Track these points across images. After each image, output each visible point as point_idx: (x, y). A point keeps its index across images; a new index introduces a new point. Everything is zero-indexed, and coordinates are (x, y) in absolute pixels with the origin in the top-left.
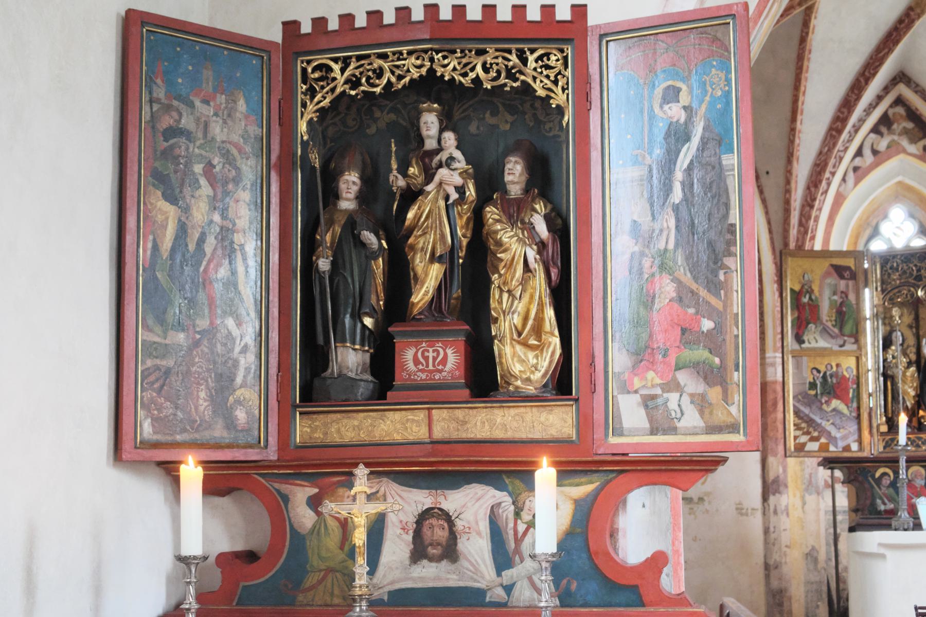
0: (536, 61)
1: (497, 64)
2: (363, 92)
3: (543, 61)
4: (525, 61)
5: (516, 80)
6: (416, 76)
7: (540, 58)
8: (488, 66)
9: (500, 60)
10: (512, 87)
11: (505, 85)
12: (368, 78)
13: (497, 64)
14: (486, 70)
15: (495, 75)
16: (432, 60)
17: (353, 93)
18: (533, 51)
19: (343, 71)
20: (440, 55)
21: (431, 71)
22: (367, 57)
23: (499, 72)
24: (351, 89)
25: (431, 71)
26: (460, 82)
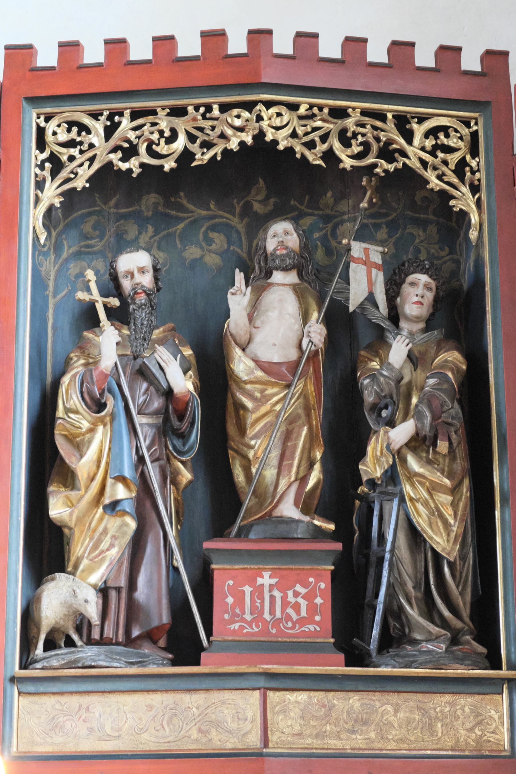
0: (427, 135)
1: (363, 135)
2: (142, 165)
3: (437, 138)
4: (409, 137)
5: (391, 160)
6: (234, 145)
7: (433, 132)
8: (349, 134)
9: (368, 130)
10: (386, 171)
11: (375, 165)
12: (151, 144)
13: (363, 135)
14: (346, 142)
15: (360, 149)
16: (259, 118)
17: (124, 166)
18: (421, 120)
19: (109, 131)
20: (273, 110)
21: (260, 135)
22: (153, 112)
23: (366, 145)
24: (124, 159)
25: (260, 135)
26: (303, 156)
